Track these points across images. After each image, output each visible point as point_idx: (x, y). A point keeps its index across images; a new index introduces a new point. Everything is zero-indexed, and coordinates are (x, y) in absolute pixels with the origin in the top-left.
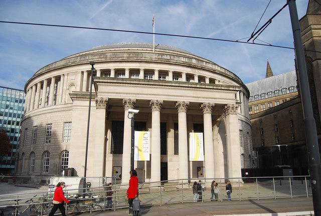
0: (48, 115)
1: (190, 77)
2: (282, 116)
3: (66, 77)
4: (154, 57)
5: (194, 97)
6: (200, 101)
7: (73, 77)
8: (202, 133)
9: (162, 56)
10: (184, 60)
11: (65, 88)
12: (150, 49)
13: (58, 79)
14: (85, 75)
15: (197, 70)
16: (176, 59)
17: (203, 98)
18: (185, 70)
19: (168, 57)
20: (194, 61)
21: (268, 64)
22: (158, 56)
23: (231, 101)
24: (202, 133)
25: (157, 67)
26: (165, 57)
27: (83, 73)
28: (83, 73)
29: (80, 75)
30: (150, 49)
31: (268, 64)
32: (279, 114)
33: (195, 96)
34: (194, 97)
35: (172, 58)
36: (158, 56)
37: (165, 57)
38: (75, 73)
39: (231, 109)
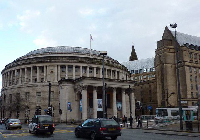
0: (38, 88)
2: (146, 88)
3: (48, 68)
7: (52, 68)
11: (48, 73)
13: (42, 68)
14: (59, 67)
18: (107, 68)
20: (110, 63)
21: (133, 46)
27: (58, 66)
28: (58, 66)
29: (56, 68)
31: (133, 46)
32: (144, 86)
38: (55, 66)
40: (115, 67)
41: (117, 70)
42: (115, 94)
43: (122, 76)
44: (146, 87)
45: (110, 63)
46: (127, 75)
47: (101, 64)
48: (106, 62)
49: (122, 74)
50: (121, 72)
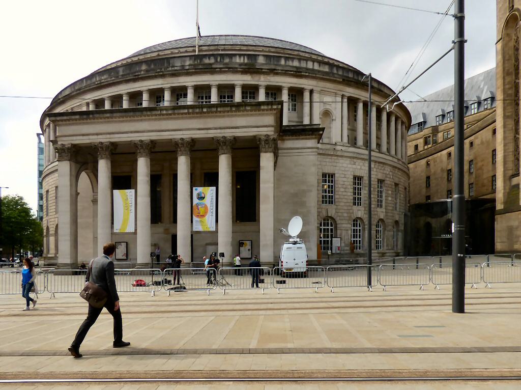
1: (250, 91)
2: (482, 143)
4: (188, 63)
5: (199, 129)
6: (212, 134)
8: (214, 188)
9: (201, 60)
10: (242, 61)
12: (191, 49)
15: (262, 78)
16: (227, 60)
17: (216, 129)
18: (239, 80)
19: (212, 61)
20: (261, 60)
22: (195, 60)
23: (265, 129)
24: (214, 188)
25: (189, 81)
26: (207, 61)
30: (191, 49)
33: (202, 126)
34: (199, 129)
35: (219, 60)
36: (195, 60)
37: (207, 61)
39: (263, 143)
40: (273, 72)
41: (286, 82)
42: (183, 165)
43: (316, 106)
44: (484, 140)
45: (261, 60)
46: (352, 102)
47: (210, 70)
48: (238, 60)
49: (316, 97)
50: (311, 92)
